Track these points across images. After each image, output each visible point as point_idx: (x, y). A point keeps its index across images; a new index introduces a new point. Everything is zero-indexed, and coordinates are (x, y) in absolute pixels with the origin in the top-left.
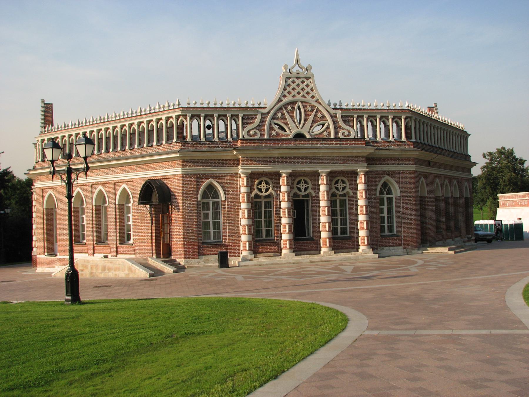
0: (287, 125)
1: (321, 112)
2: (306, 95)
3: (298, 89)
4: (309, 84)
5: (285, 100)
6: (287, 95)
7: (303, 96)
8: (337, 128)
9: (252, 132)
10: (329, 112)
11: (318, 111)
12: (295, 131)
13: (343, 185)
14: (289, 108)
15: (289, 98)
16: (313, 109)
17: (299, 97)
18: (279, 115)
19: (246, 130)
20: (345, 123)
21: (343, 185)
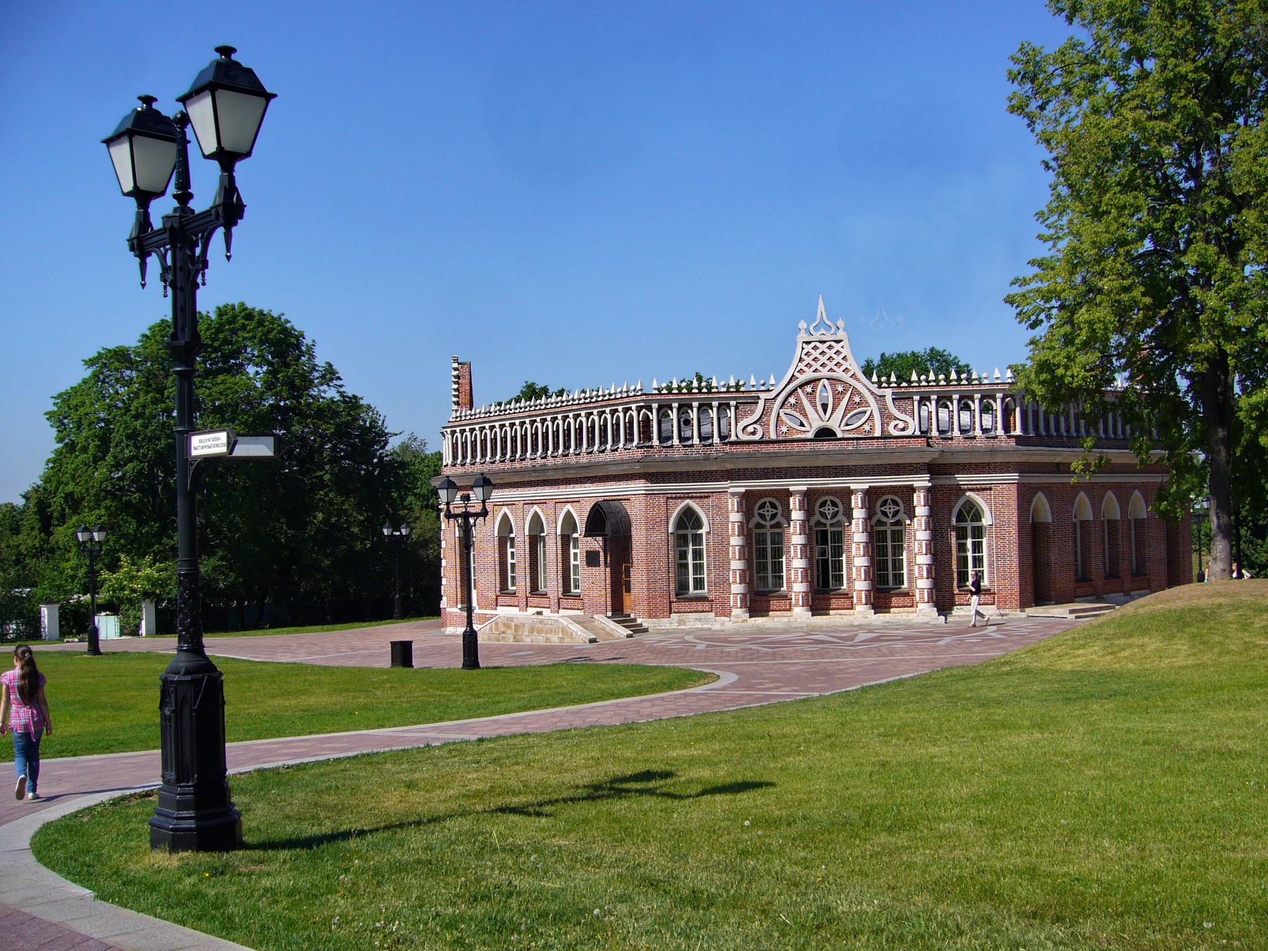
0: (806, 416)
1: (859, 393)
2: (835, 368)
3: (823, 359)
4: (841, 350)
5: (802, 378)
6: (805, 369)
7: (831, 370)
8: (886, 417)
9: (750, 429)
10: (872, 393)
11: (856, 392)
12: (815, 422)
13: (894, 508)
14: (809, 389)
15: (809, 374)
16: (845, 390)
17: (824, 372)
18: (792, 400)
19: (741, 425)
20: (899, 410)
21: (894, 508)
